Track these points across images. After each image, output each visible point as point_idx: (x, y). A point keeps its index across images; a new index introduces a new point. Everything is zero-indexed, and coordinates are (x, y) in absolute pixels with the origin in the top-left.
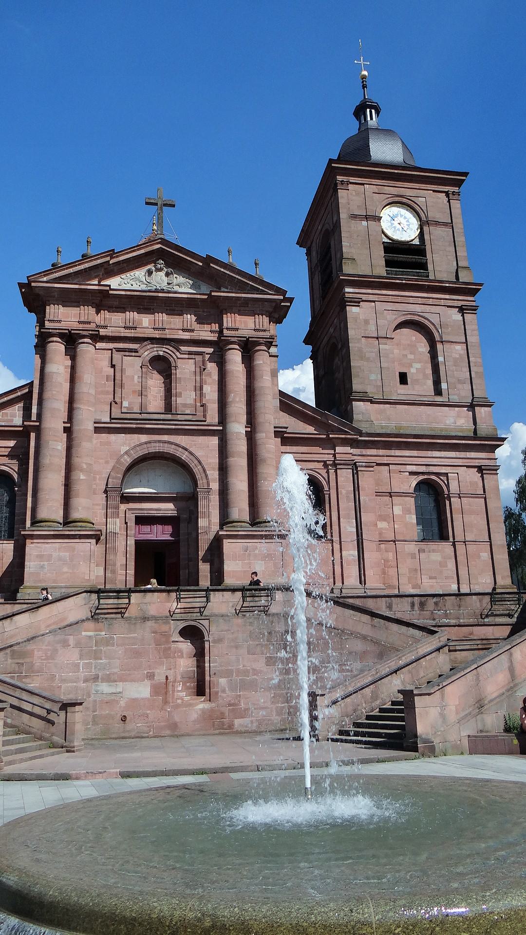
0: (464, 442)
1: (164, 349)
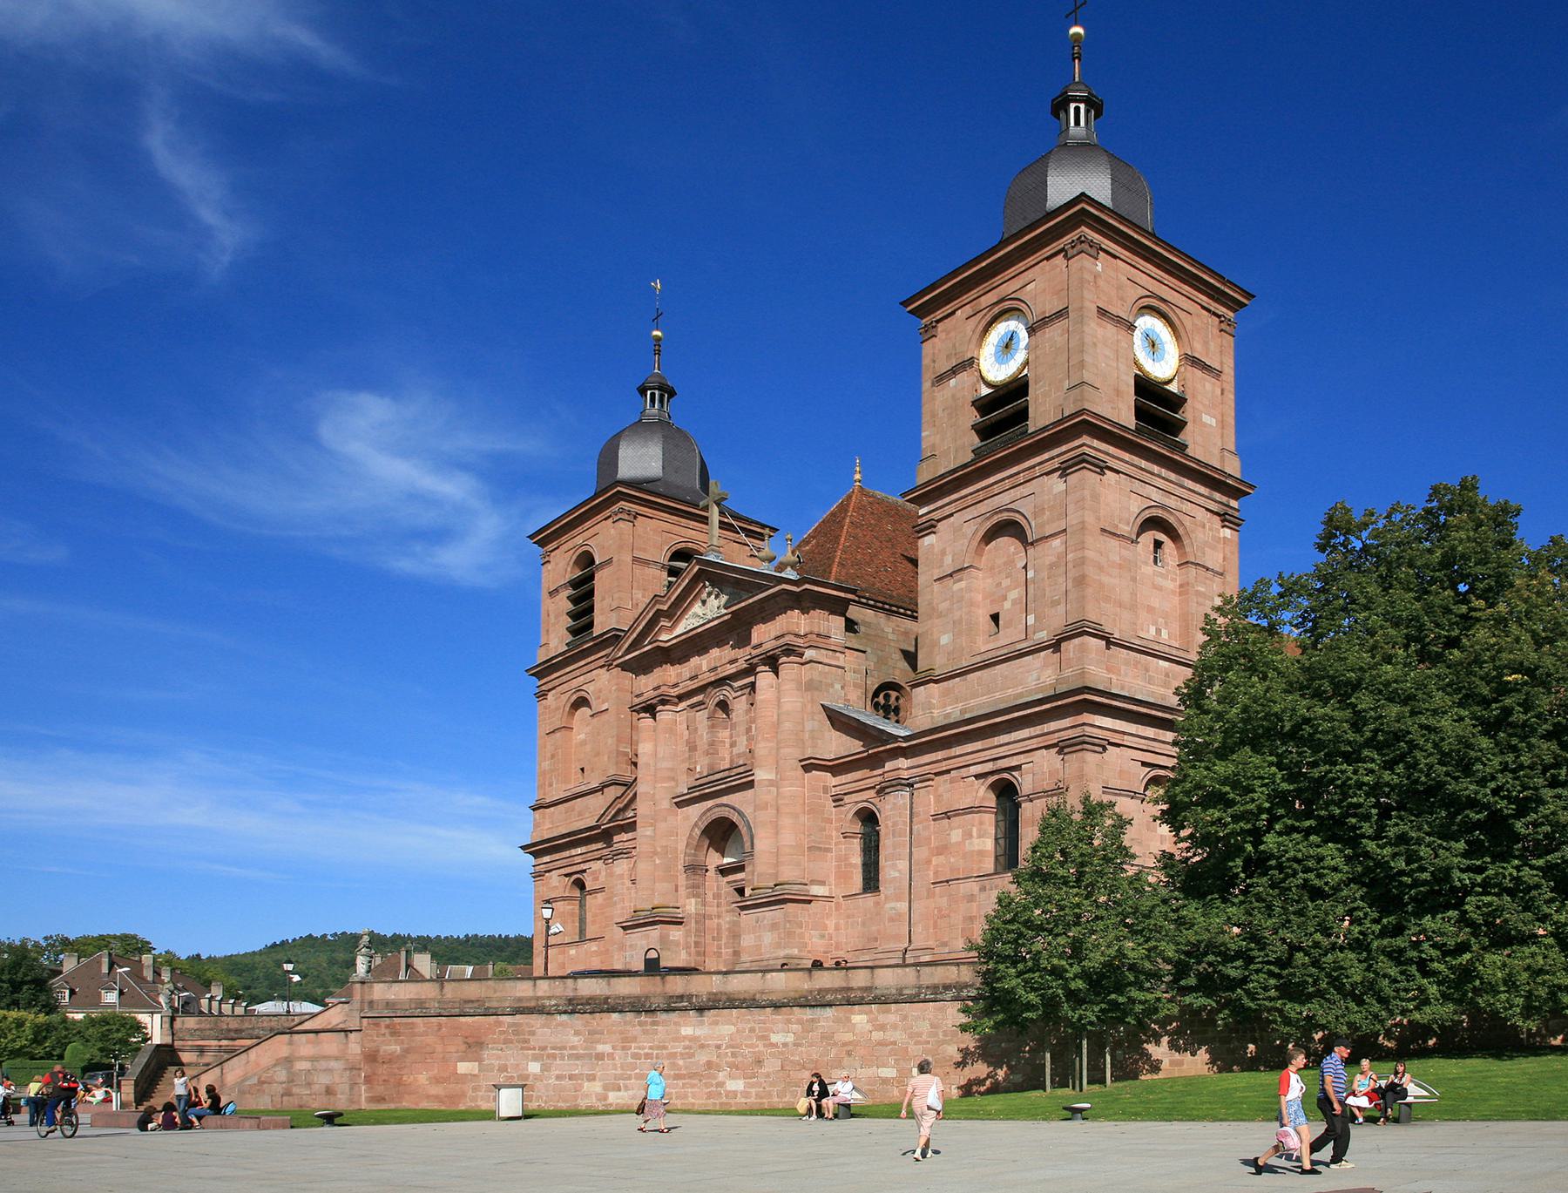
0: (1029, 711)
1: (724, 692)
